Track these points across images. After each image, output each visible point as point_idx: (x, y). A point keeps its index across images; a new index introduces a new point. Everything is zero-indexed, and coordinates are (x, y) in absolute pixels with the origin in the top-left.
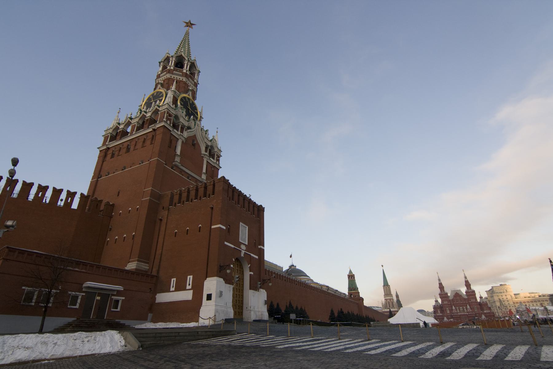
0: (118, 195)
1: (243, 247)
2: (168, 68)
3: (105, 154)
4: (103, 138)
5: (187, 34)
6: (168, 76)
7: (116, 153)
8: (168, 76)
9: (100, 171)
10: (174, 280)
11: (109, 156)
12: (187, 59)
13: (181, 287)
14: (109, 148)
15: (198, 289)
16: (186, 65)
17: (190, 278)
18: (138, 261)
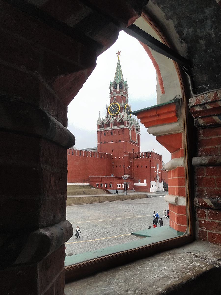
0: (113, 151)
1: (158, 171)
2: (117, 90)
3: (100, 133)
4: (97, 126)
5: (119, 61)
6: (118, 95)
7: (106, 134)
8: (118, 95)
9: (101, 141)
10: (139, 180)
11: (103, 135)
12: (124, 84)
13: (142, 182)
14: (102, 131)
15: (149, 184)
16: (124, 87)
17: (145, 180)
18: (128, 174)
